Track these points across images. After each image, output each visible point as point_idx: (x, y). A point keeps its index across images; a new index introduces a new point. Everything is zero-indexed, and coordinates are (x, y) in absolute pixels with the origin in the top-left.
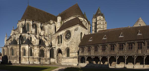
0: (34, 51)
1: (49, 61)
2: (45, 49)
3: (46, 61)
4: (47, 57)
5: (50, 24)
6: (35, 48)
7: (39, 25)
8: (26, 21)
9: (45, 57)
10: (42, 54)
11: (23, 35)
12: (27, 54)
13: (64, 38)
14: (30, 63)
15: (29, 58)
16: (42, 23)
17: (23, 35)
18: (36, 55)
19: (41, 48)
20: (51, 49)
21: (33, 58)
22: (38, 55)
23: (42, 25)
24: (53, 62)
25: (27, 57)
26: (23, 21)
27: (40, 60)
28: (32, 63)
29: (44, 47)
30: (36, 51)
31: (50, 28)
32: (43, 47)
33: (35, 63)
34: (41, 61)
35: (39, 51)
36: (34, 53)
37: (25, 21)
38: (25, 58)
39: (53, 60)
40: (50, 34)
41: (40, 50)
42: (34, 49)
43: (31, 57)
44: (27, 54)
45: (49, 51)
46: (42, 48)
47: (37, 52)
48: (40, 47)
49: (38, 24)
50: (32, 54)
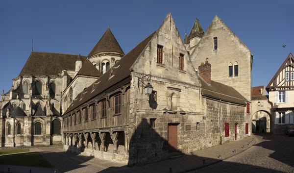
0: (23, 125)
1: (49, 140)
2: (42, 121)
3: (44, 140)
4: (45, 133)
5: (59, 77)
6: (25, 122)
7: (45, 80)
8: (23, 79)
9: (42, 135)
10: (36, 129)
11: (12, 101)
12: (12, 132)
13: (69, 100)
14: (17, 145)
15: (14, 138)
16: (50, 76)
17: (12, 101)
18: (26, 132)
19: (35, 120)
20: (54, 119)
21: (22, 137)
22: (29, 132)
23: (51, 80)
24: (58, 142)
25: (11, 136)
26: (19, 79)
27: (32, 139)
28: (19, 145)
29: (41, 118)
30: (26, 125)
31: (60, 84)
32: (40, 119)
33: (25, 144)
34: (35, 141)
35: (30, 125)
36: (23, 129)
37: (22, 78)
38: (9, 138)
39: (58, 137)
40: (60, 94)
41: (32, 124)
42: (24, 123)
43: (18, 135)
44: (12, 132)
45: (49, 124)
46: (37, 119)
47: (27, 128)
48: (33, 118)
49: (43, 79)
50: (20, 130)
